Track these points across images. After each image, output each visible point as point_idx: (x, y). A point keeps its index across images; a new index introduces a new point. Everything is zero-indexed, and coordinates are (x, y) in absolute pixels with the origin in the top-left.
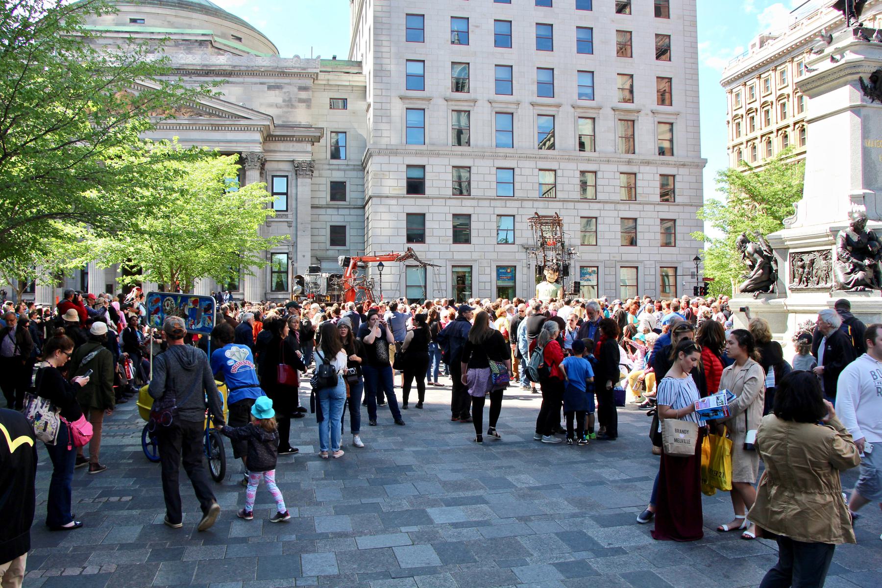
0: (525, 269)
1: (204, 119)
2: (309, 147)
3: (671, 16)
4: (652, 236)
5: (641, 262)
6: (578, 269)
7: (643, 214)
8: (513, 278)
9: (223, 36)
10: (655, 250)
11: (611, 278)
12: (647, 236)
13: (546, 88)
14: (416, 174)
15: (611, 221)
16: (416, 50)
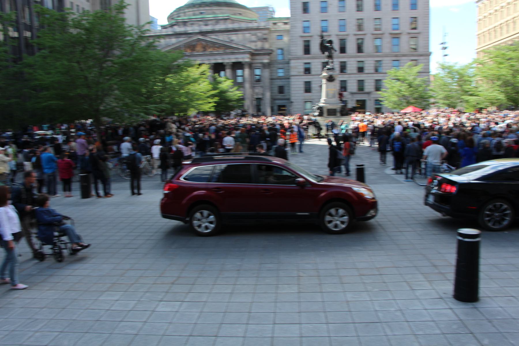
1: (228, 51)
2: (267, 57)
9: (235, 14)
13: (360, 27)
14: (307, 66)
16: (306, 16)
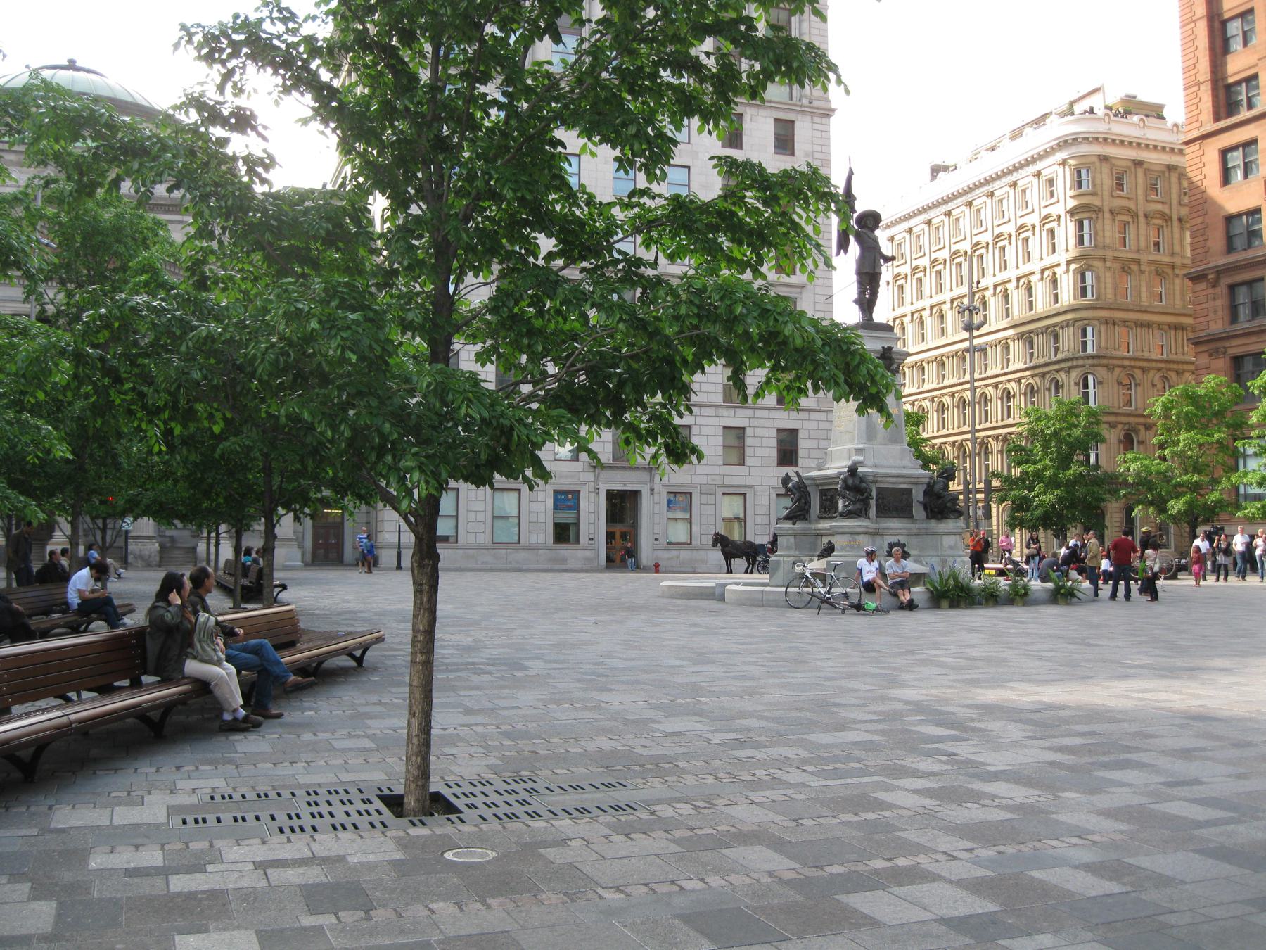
0: (592, 495)
3: (797, 153)
4: (765, 452)
5: (750, 487)
6: (664, 495)
7: (754, 422)
8: (577, 508)
10: (769, 471)
11: (710, 509)
12: (759, 452)
15: (710, 431)
